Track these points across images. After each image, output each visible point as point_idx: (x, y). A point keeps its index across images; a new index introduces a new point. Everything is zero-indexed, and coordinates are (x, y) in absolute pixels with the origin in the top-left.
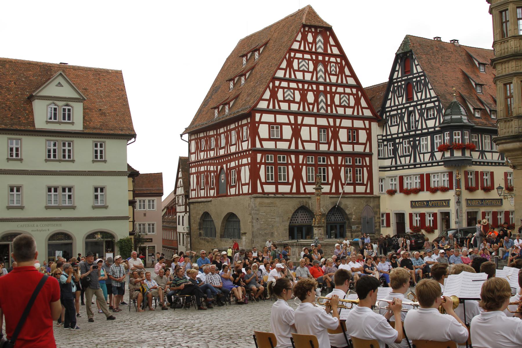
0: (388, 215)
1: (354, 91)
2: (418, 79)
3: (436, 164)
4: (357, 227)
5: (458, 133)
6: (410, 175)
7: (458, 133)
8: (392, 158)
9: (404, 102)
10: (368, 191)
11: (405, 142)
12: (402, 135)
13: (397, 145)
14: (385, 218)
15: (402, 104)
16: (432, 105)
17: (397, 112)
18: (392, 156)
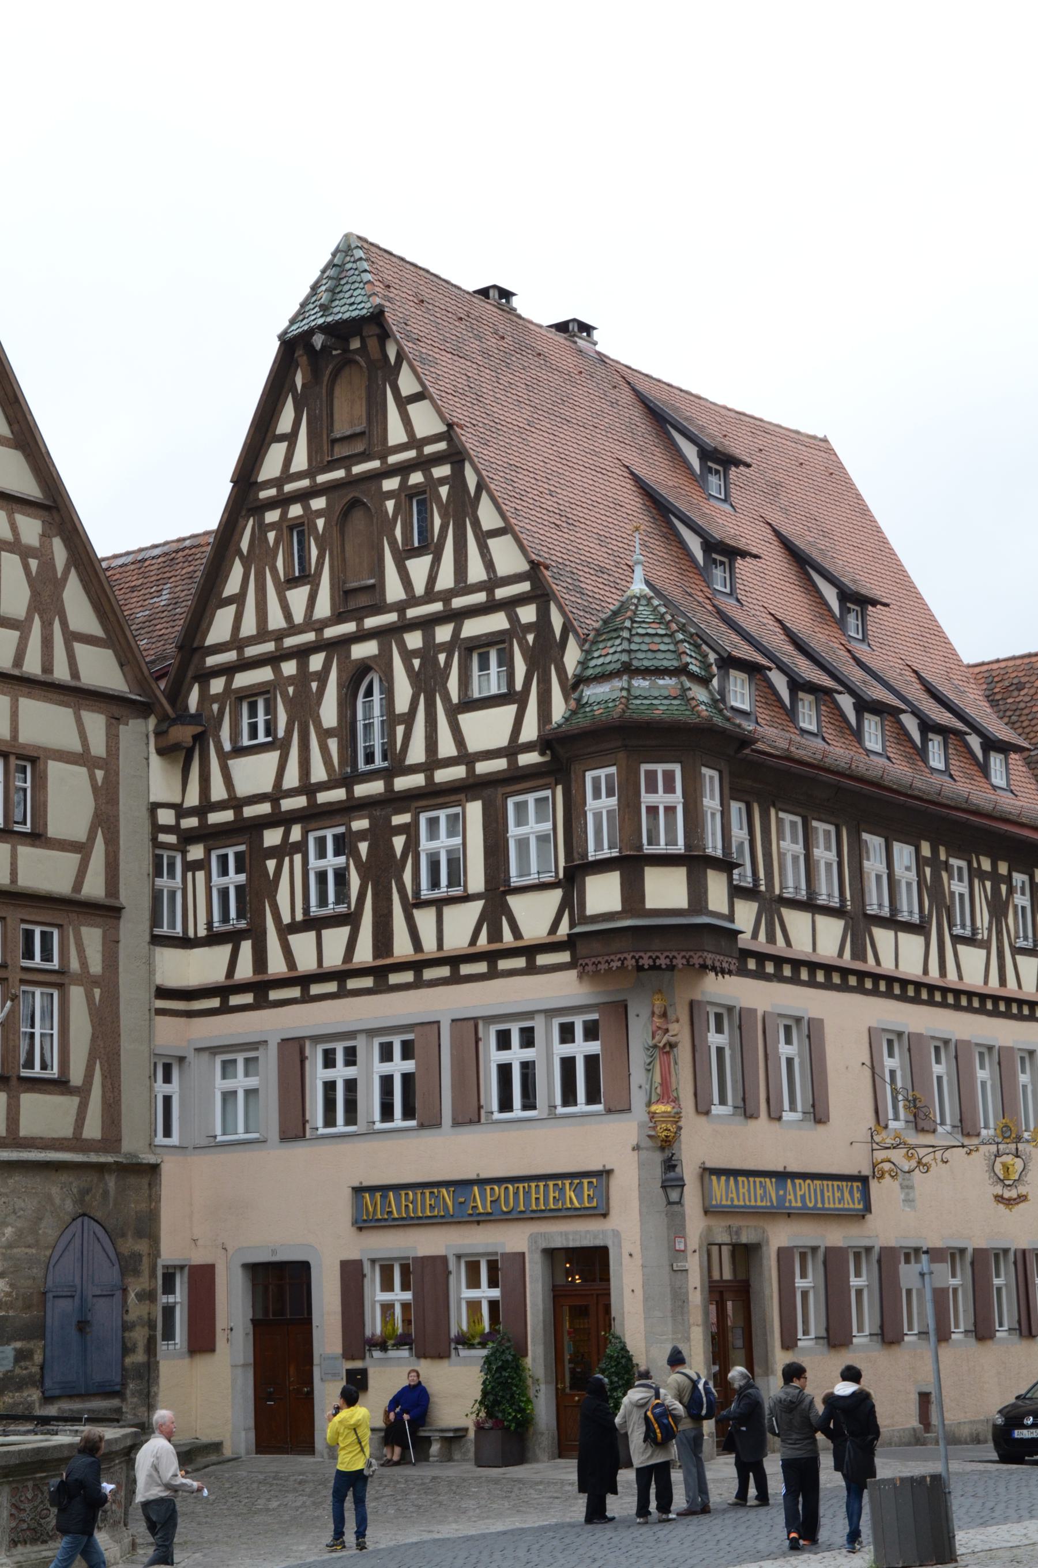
0: (202, 1279)
1: (30, 529)
2: (416, 478)
3: (520, 962)
4: (21, 1356)
5: (669, 776)
6: (352, 1035)
7: (669, 776)
8: (233, 938)
9: (323, 609)
10: (93, 1130)
11: (321, 842)
12: (300, 802)
13: (271, 864)
14: (179, 1297)
15: (310, 624)
16: (498, 622)
17: (277, 671)
18: (236, 923)
